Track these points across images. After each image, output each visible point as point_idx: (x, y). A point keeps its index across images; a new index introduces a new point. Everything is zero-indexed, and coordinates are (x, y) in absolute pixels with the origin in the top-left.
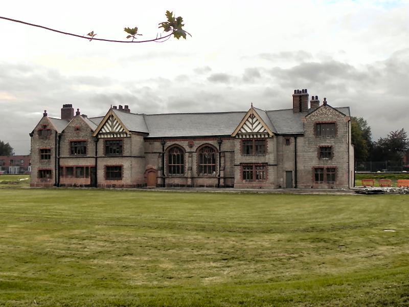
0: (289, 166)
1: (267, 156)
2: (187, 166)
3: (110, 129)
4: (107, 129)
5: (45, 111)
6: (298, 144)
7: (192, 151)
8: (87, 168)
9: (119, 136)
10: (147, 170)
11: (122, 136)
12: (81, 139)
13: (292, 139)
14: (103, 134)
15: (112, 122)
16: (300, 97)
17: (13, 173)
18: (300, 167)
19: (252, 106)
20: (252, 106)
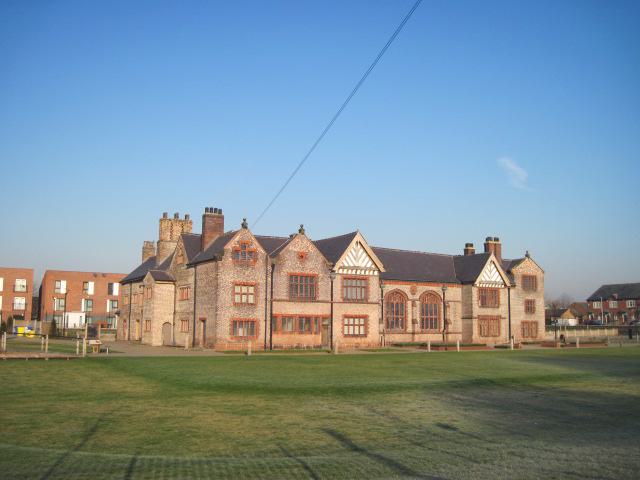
5: (245, 220)
8: (317, 317)
9: (363, 273)
11: (367, 273)
12: (307, 272)
17: (327, 333)
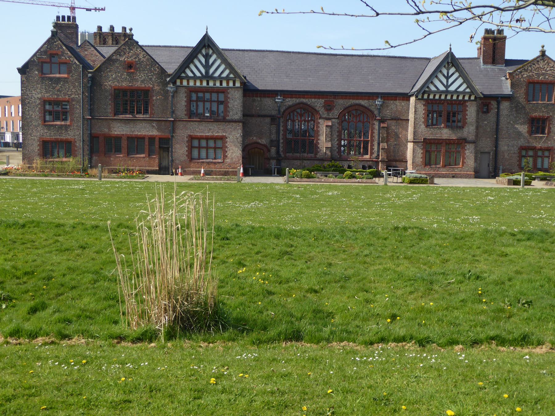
0: (486, 144)
1: (466, 130)
3: (203, 71)
4: (197, 68)
6: (501, 113)
10: (247, 145)
12: (138, 85)
13: (494, 103)
14: (188, 78)
15: (207, 57)
16: (495, 39)
18: (503, 147)
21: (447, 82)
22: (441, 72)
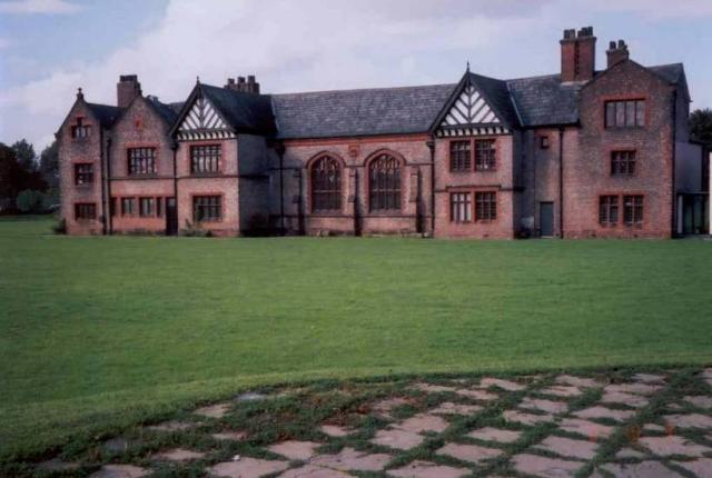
2: (348, 192)
5: (80, 89)
7: (357, 163)
8: (159, 199)
12: (146, 143)
15: (202, 108)
16: (577, 43)
19: (468, 69)
20: (468, 69)
21: (469, 113)
22: (462, 101)
